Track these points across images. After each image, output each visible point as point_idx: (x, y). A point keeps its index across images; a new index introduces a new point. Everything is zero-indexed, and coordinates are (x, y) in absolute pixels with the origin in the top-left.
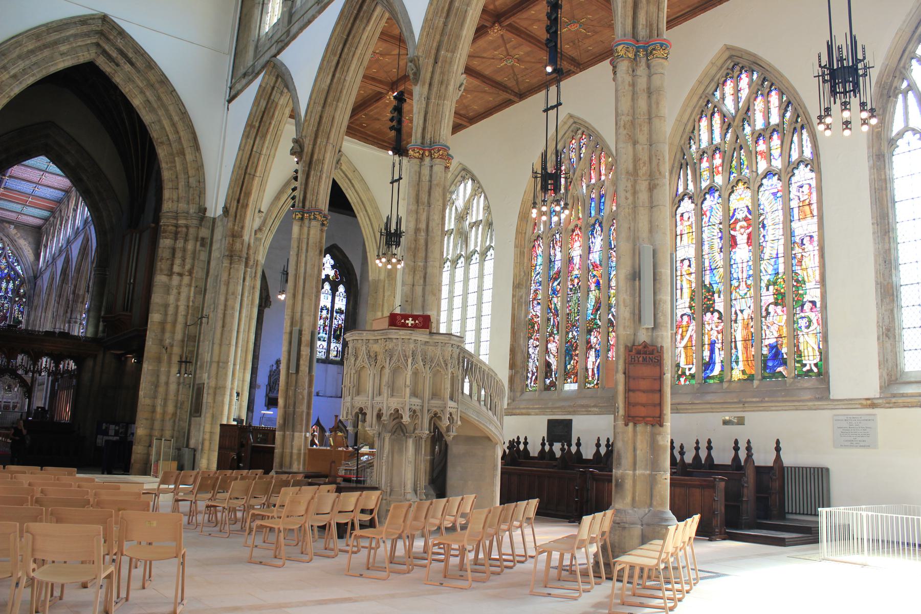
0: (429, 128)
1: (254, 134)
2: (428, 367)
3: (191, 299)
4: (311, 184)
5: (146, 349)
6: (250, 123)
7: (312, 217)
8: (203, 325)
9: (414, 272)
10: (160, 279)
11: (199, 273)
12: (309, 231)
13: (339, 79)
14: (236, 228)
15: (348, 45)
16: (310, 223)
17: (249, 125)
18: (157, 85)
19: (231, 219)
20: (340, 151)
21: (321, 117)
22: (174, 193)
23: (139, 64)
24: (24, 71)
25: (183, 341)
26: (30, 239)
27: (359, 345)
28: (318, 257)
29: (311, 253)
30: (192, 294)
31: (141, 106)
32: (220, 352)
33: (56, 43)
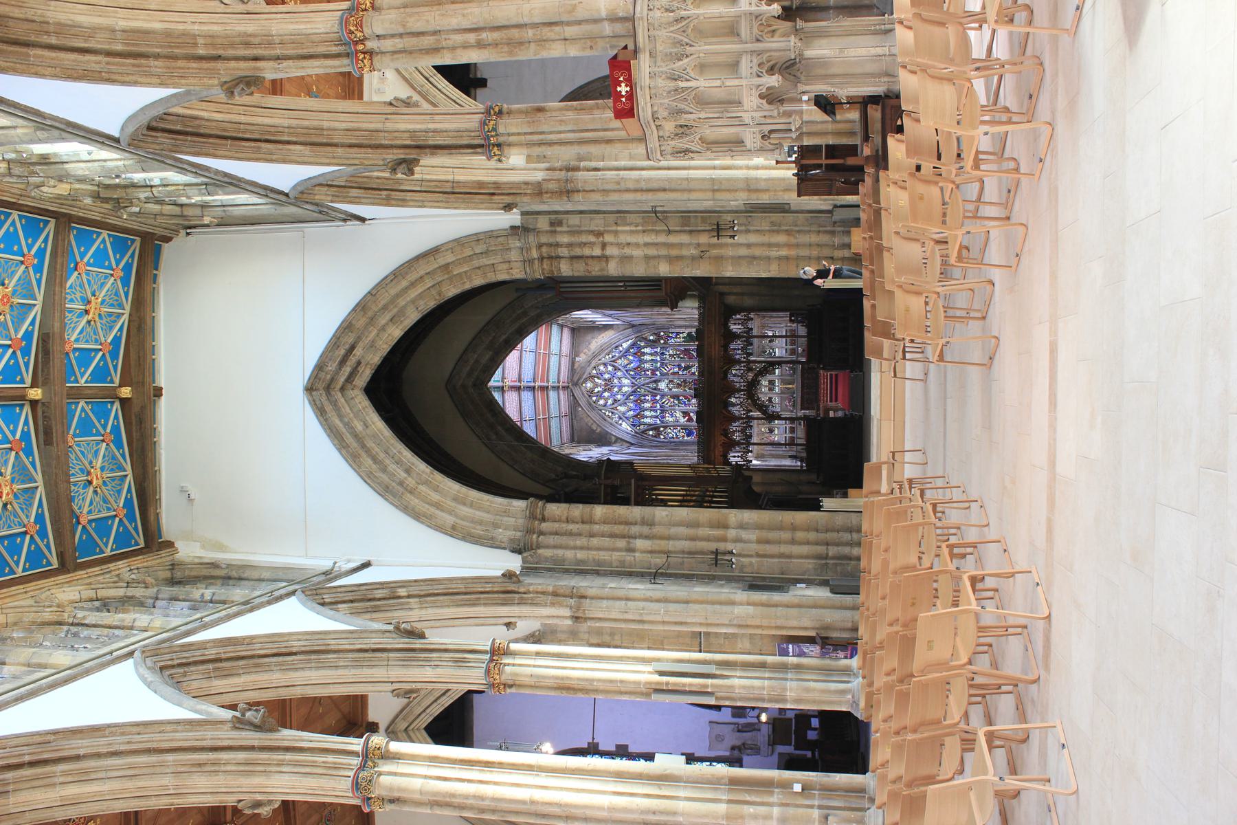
0: (321, 49)
1: (397, 193)
2: (689, 50)
3: (633, 228)
4: (448, 142)
5: (706, 275)
6: (384, 202)
7: (493, 134)
8: (665, 209)
9: (544, 41)
10: (613, 269)
11: (597, 223)
12: (513, 134)
13: (290, 134)
14: (529, 191)
15: (240, 135)
16: (503, 134)
17: (388, 202)
18: (370, 314)
19: (518, 199)
20: (391, 104)
21: (351, 146)
22: (499, 268)
23: (350, 339)
24: (399, 462)
25: (691, 232)
26: (589, 337)
27: (668, 149)
28: (548, 114)
29: (545, 128)
30: (627, 228)
31: (401, 327)
32: (701, 190)
33: (356, 436)
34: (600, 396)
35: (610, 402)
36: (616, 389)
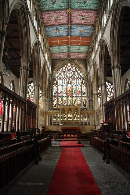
26: (83, 64)
34: (66, 67)
35: (64, 70)
36: (68, 72)
